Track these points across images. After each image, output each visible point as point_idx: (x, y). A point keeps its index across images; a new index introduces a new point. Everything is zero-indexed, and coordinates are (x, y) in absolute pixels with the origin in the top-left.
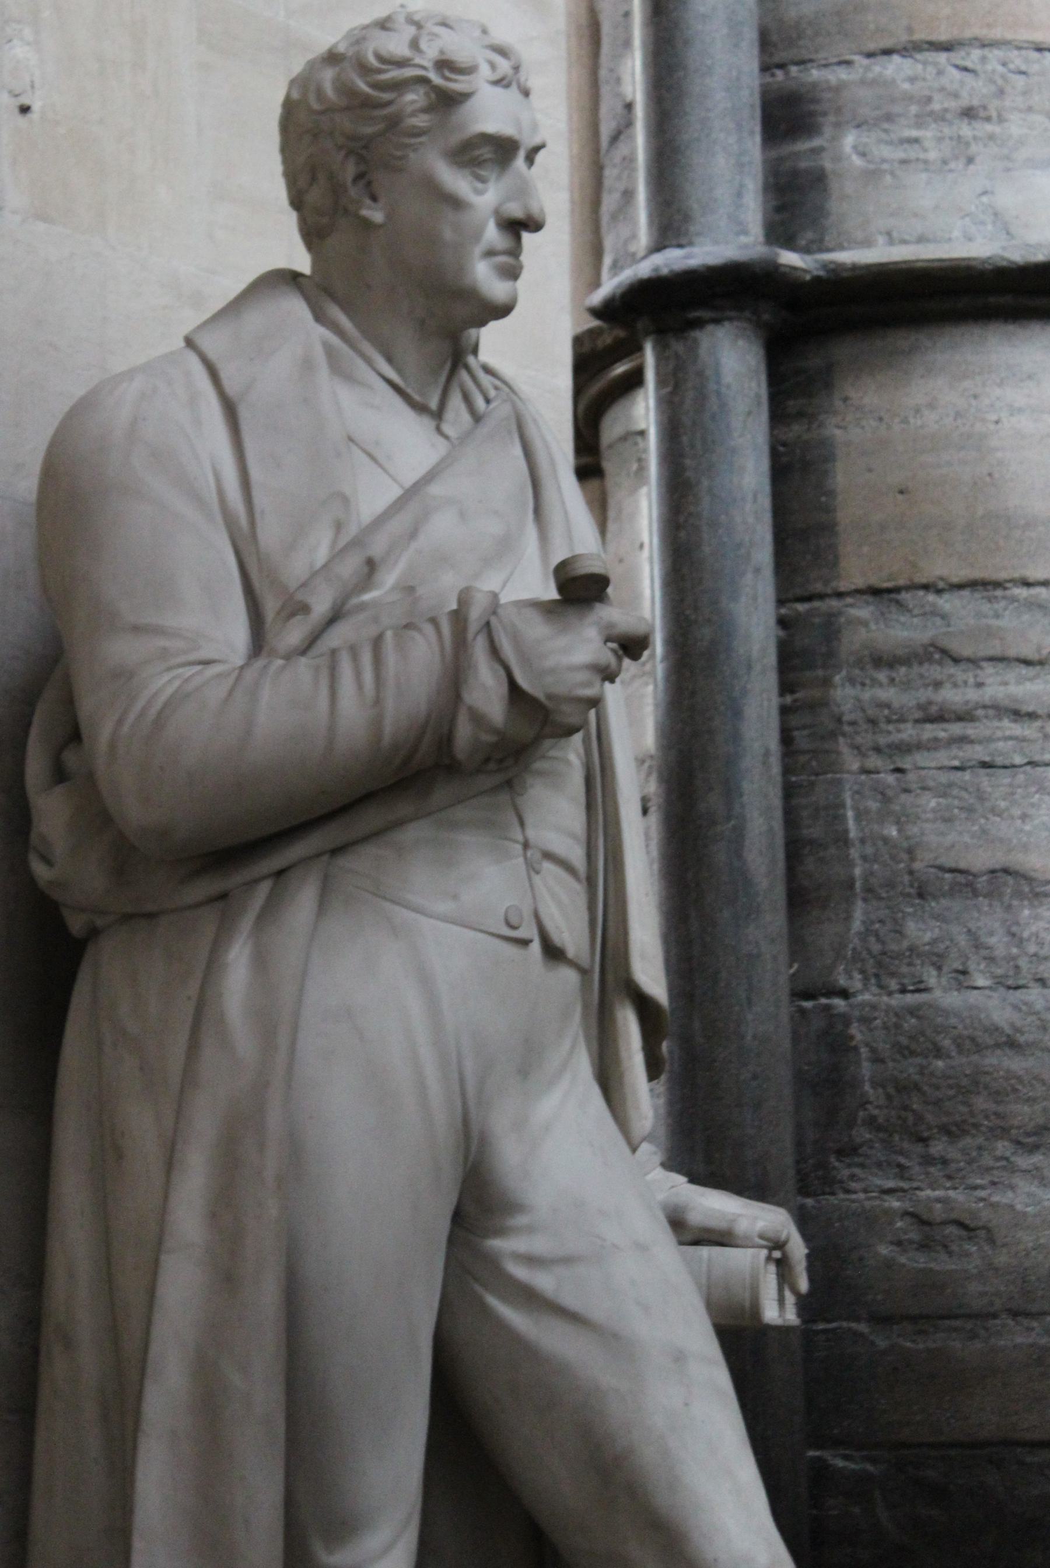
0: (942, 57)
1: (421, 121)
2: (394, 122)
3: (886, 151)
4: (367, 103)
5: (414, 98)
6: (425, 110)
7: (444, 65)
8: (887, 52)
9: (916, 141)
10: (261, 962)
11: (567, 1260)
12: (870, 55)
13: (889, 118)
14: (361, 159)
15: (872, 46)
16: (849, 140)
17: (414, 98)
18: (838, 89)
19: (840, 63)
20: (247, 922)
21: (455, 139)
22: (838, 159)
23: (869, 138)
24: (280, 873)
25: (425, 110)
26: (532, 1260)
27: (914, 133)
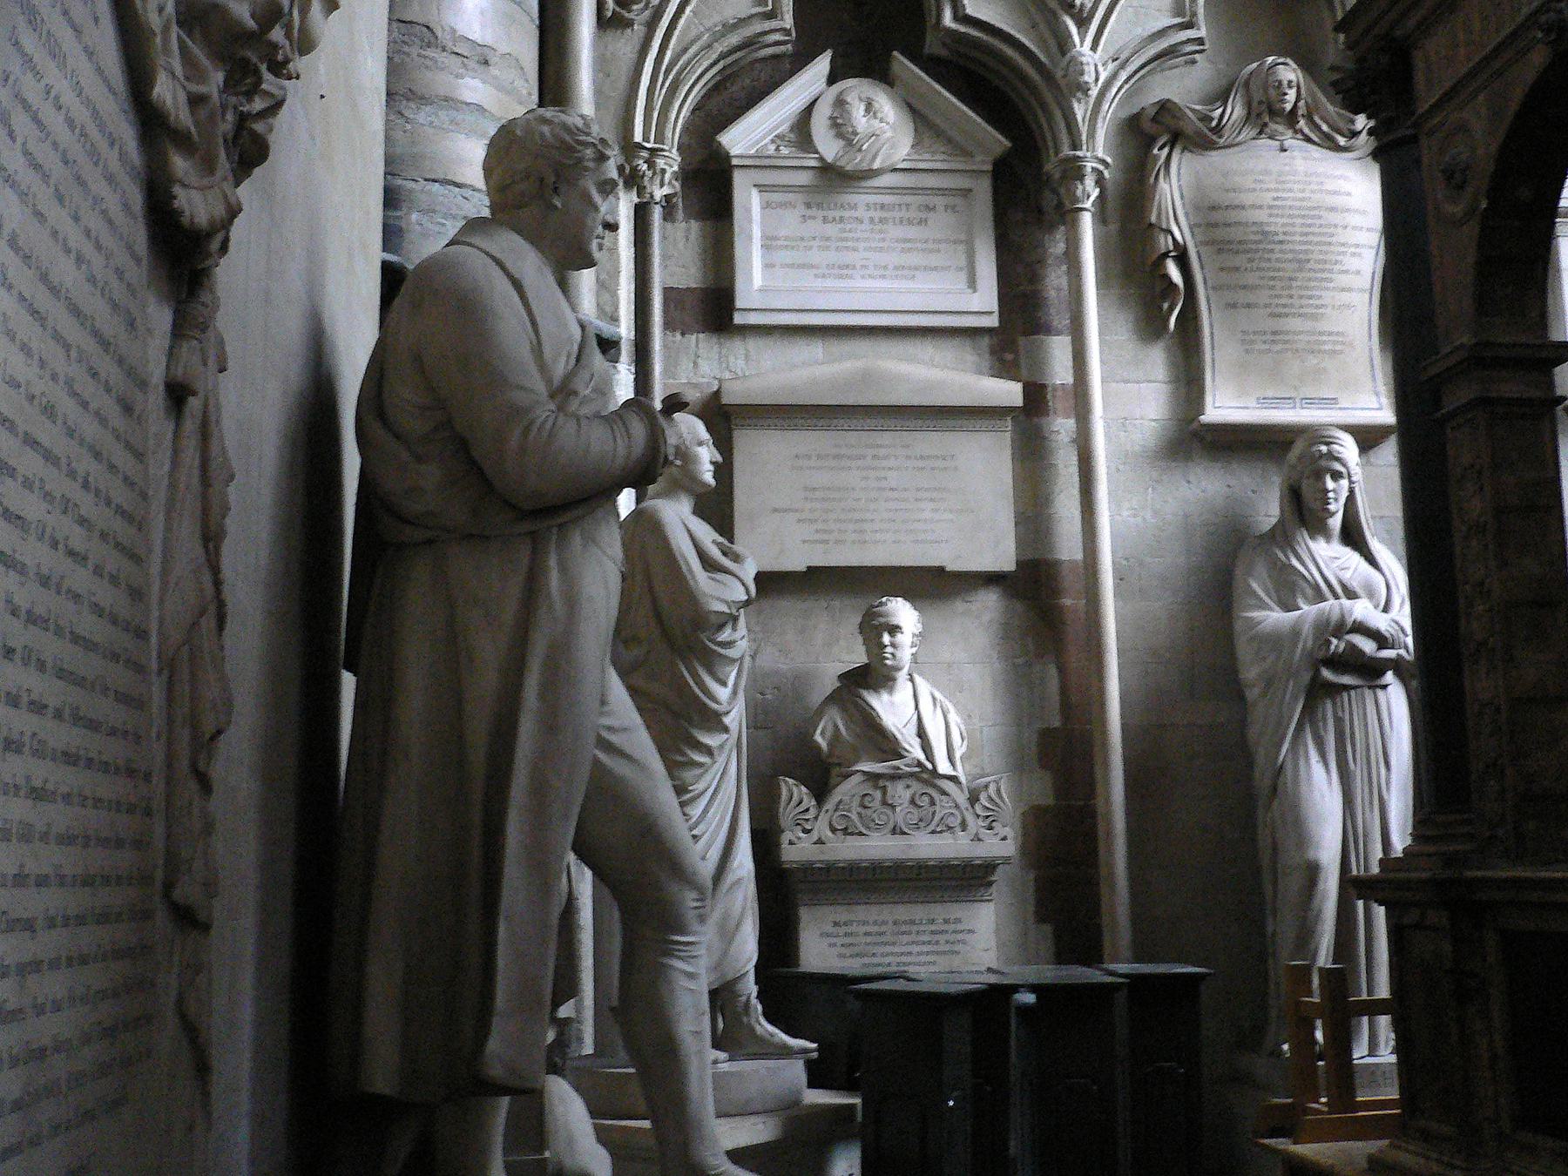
0: (457, 189)
1: (591, 165)
2: (580, 160)
3: (430, 226)
4: (571, 149)
5: (589, 152)
6: (594, 160)
7: (603, 141)
8: (435, 181)
9: (444, 225)
10: (564, 569)
11: (625, 729)
12: (426, 180)
13: (434, 211)
14: (558, 176)
15: (428, 177)
16: (414, 217)
17: (589, 152)
18: (411, 191)
19: (413, 180)
20: (553, 547)
21: (603, 178)
22: (408, 224)
23: (425, 220)
24: (560, 526)
25: (594, 160)
26: (610, 729)
27: (444, 221)
